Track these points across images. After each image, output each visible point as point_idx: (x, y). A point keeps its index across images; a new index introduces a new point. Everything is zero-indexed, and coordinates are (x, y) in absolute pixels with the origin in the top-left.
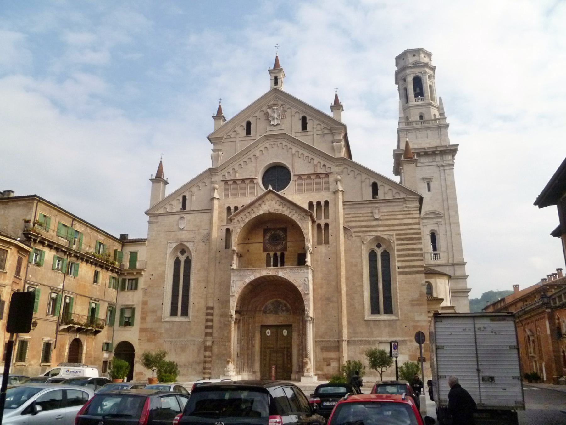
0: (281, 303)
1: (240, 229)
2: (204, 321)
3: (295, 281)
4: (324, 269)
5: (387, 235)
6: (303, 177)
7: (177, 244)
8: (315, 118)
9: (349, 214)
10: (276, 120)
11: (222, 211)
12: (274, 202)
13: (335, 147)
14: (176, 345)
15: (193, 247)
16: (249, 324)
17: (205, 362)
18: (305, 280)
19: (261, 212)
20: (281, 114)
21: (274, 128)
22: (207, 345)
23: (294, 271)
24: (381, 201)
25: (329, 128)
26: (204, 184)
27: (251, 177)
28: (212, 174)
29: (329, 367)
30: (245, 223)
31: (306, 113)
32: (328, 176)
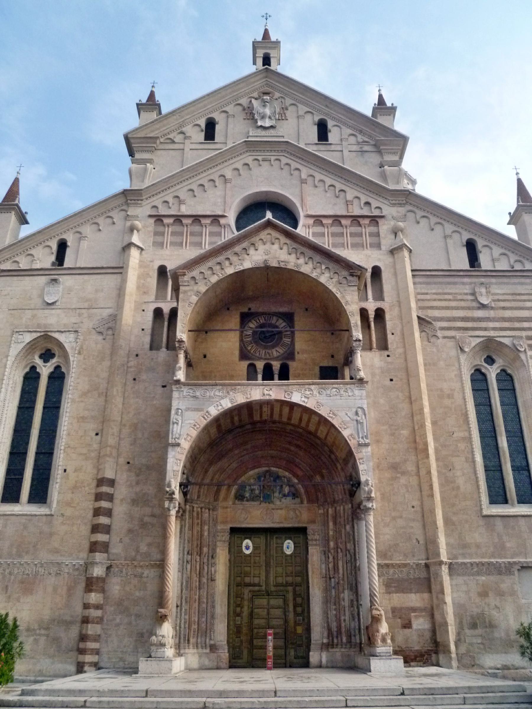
0: (278, 477)
1: (196, 295)
2: (91, 513)
3: (334, 414)
4: (382, 401)
5: (509, 337)
6: (325, 221)
7: (35, 335)
8: (345, 124)
9: (427, 294)
10: (267, 120)
11: (148, 274)
12: (276, 246)
13: (388, 173)
14: (10, 574)
15: (74, 344)
16: (202, 524)
17: (85, 621)
18: (357, 414)
19: (247, 265)
20: (278, 110)
21: (263, 133)
22: (95, 575)
23: (328, 392)
24: (489, 274)
25: (373, 143)
26: (109, 221)
27: (213, 214)
28: (129, 201)
29: (407, 631)
30: (210, 285)
31: (327, 114)
32: (377, 223)
